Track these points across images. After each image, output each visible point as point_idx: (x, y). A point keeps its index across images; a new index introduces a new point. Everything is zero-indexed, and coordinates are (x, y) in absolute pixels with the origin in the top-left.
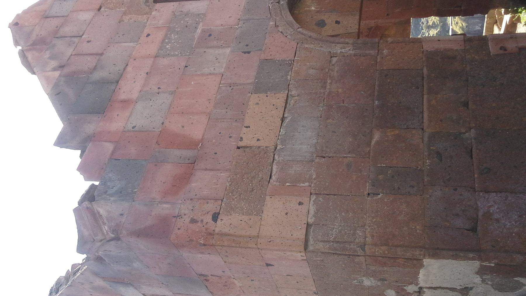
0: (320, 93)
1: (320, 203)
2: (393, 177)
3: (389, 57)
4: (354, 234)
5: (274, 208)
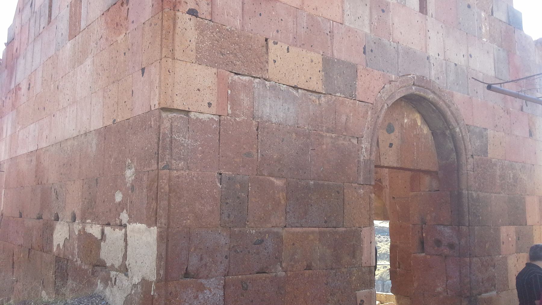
0: (322, 127)
1: (211, 125)
2: (238, 198)
3: (356, 195)
4: (180, 159)
5: (204, 77)
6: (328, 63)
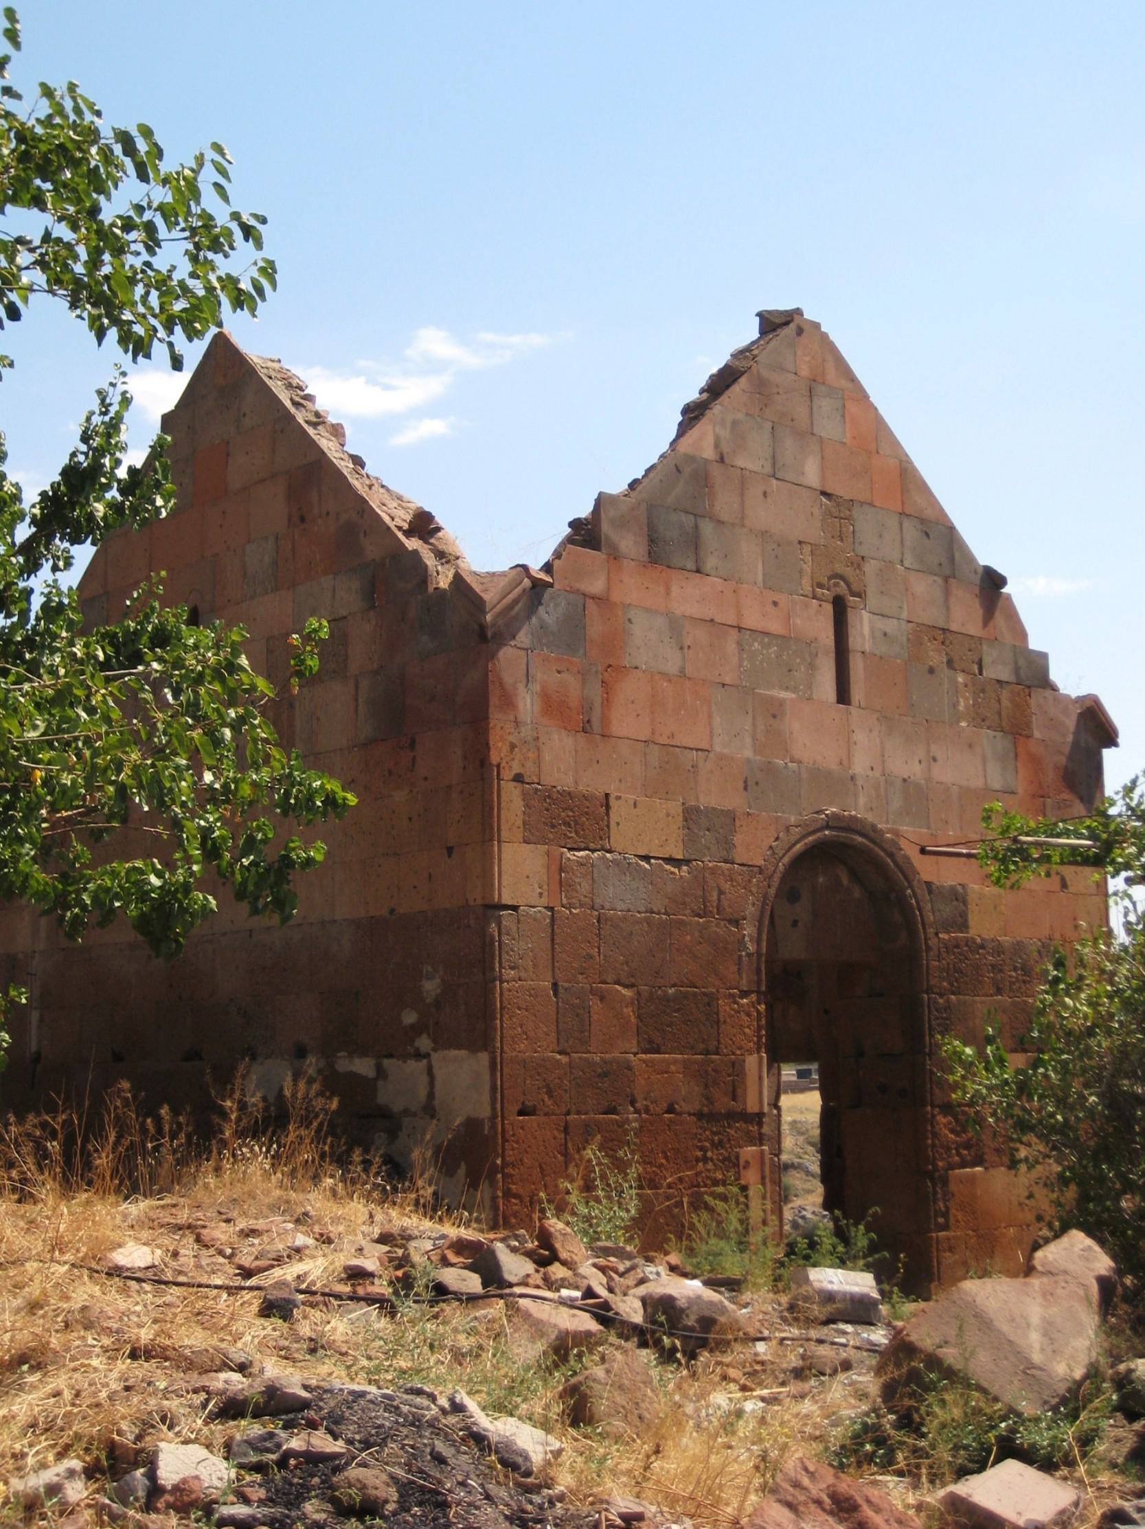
4: (512, 968)
6: (690, 814)
